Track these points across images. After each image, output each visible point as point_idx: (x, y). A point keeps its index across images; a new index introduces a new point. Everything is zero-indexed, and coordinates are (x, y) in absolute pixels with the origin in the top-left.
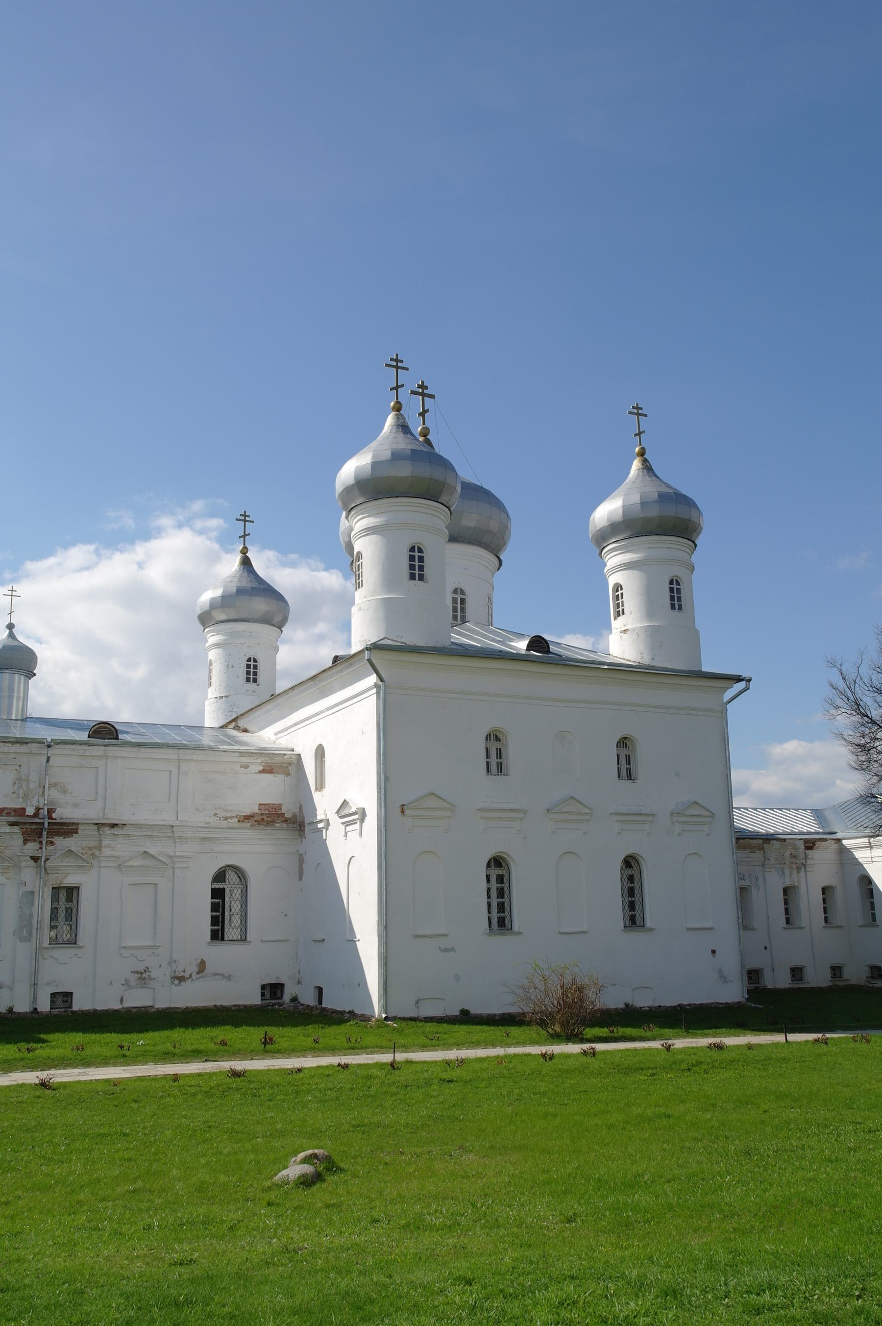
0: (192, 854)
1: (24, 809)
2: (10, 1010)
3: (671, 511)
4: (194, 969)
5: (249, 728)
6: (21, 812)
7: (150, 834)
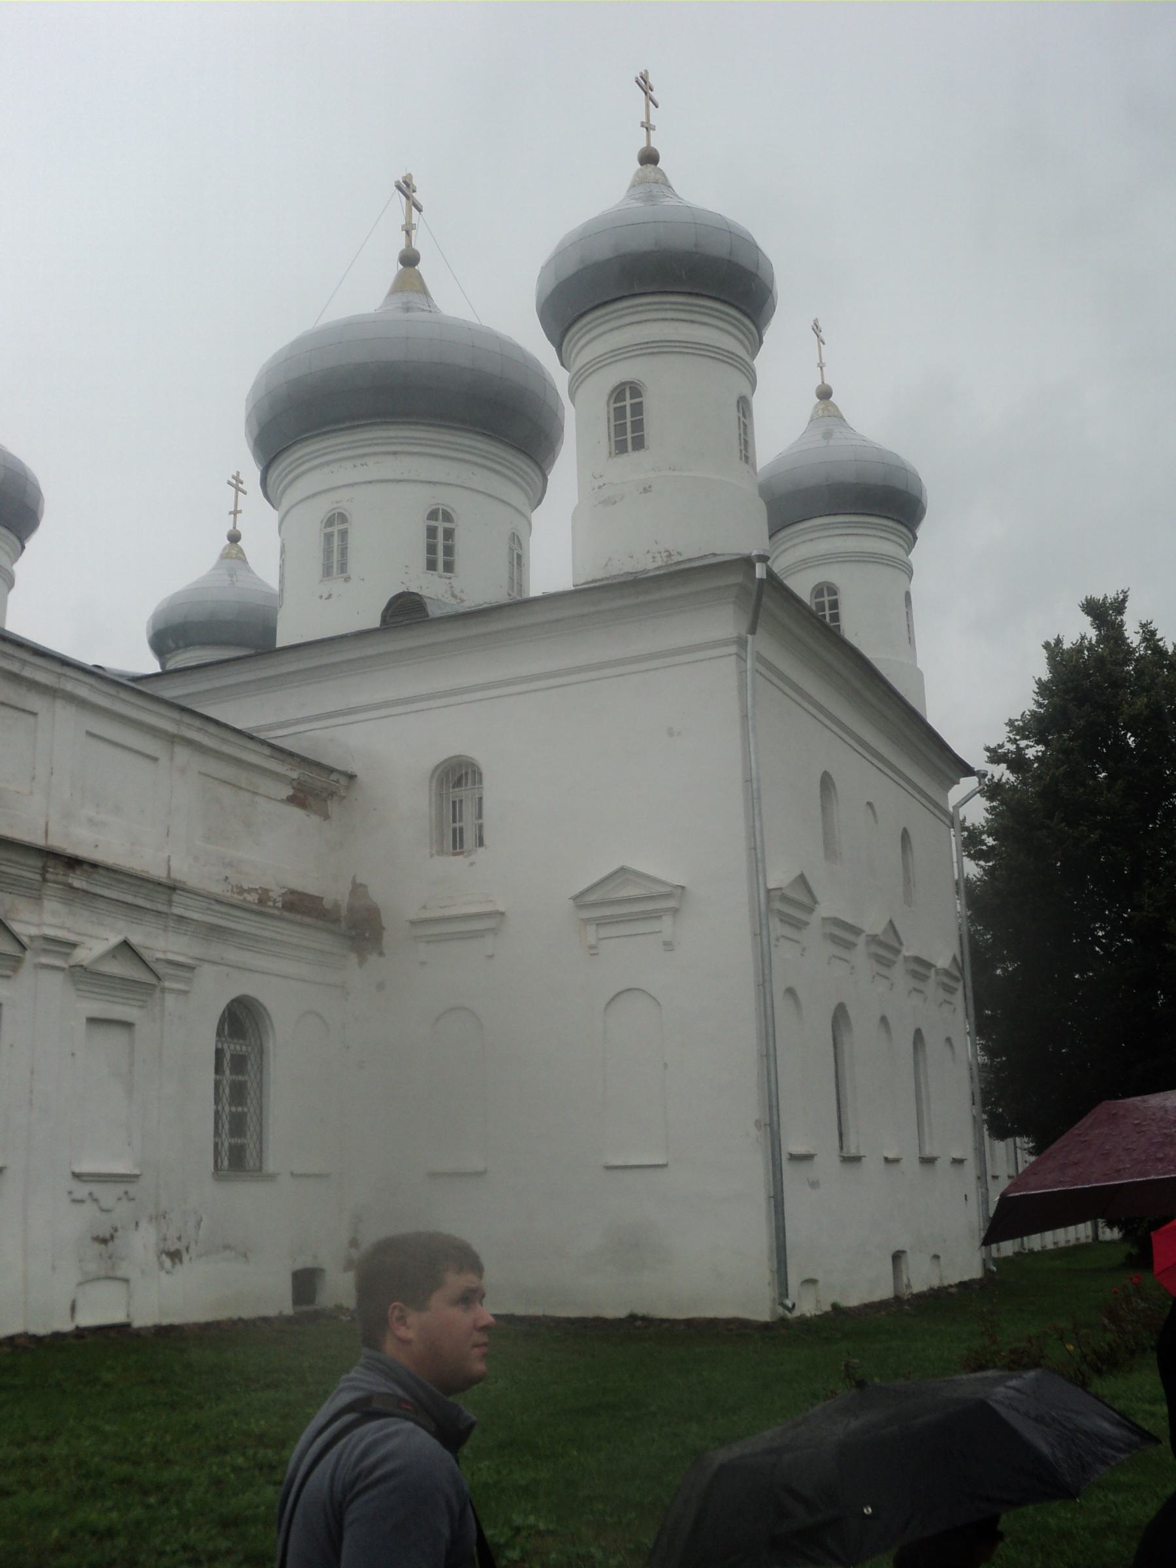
0: (190, 961)
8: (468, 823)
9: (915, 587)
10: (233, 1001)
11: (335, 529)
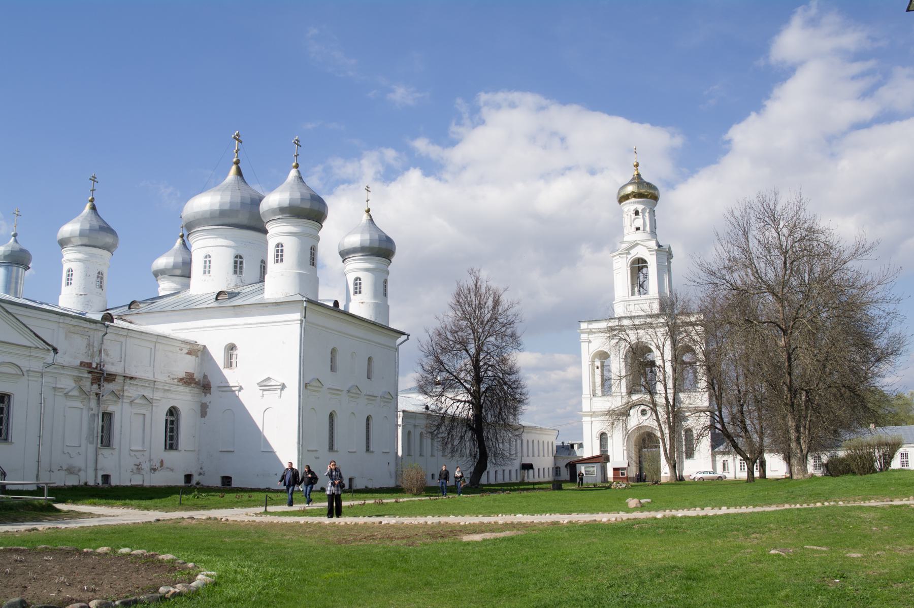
1: (91, 364)
2: (86, 484)
3: (384, 246)
4: (158, 465)
5: (133, 321)
6: (89, 365)
7: (144, 385)
8: (234, 360)
9: (389, 278)
10: (172, 407)
11: (208, 259)
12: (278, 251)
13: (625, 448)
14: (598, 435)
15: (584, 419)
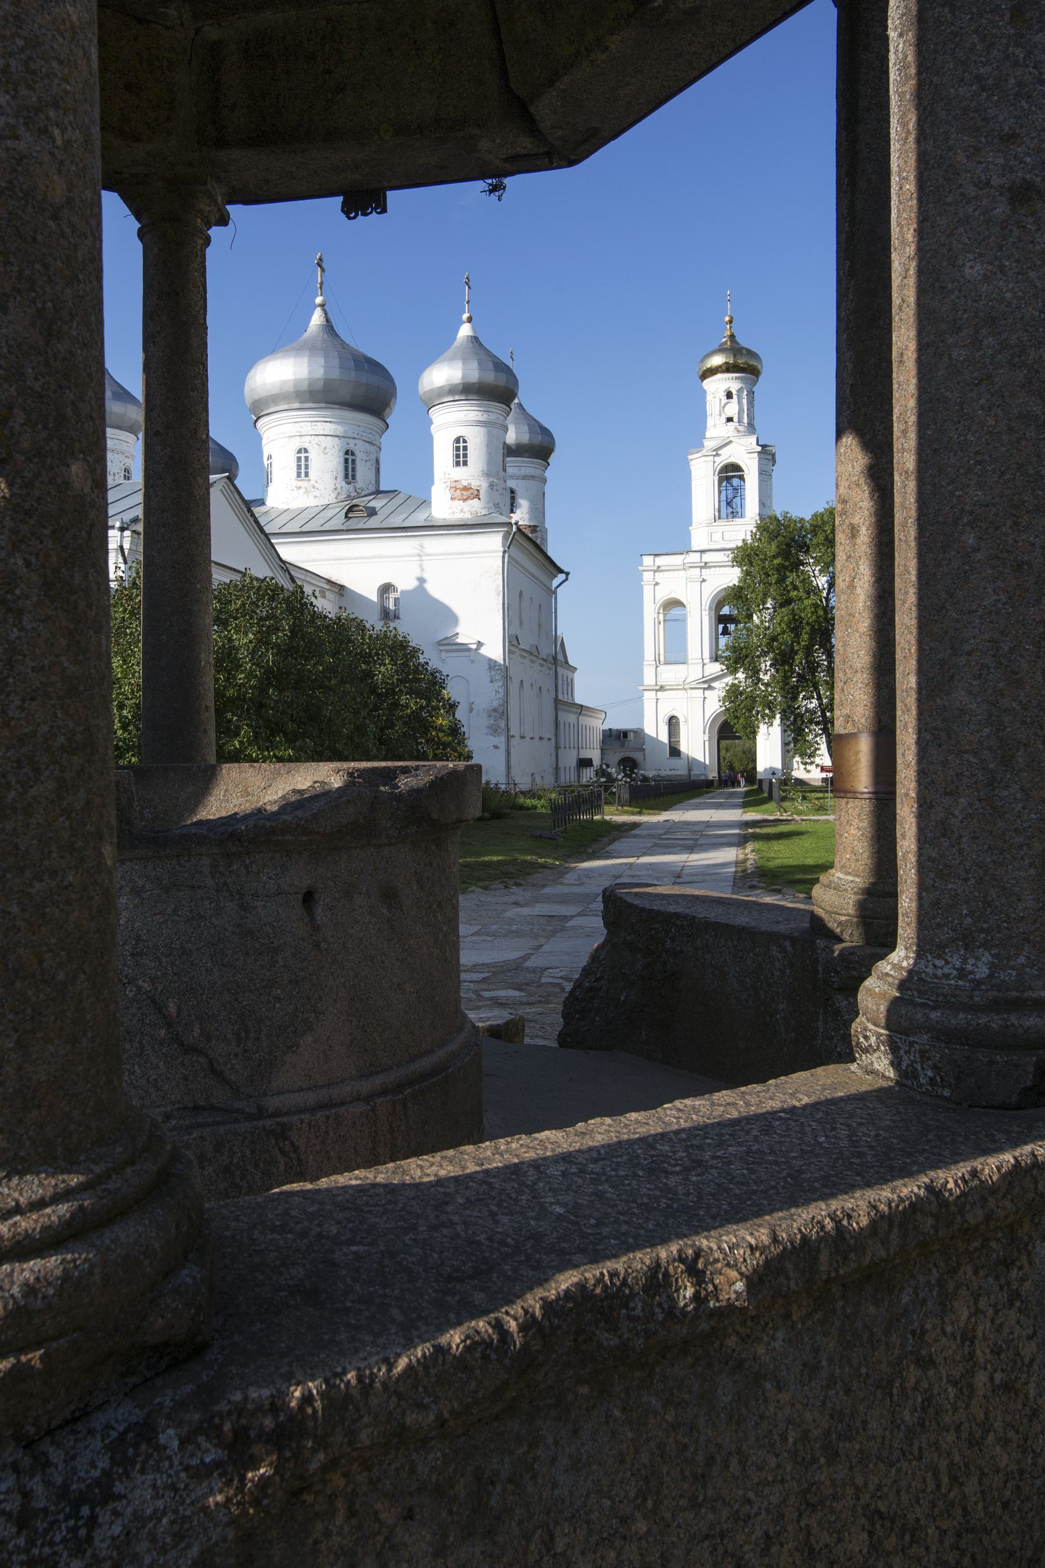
9: (547, 488)
11: (303, 455)
12: (458, 449)
13: (707, 738)
14: (666, 720)
15: (647, 694)
